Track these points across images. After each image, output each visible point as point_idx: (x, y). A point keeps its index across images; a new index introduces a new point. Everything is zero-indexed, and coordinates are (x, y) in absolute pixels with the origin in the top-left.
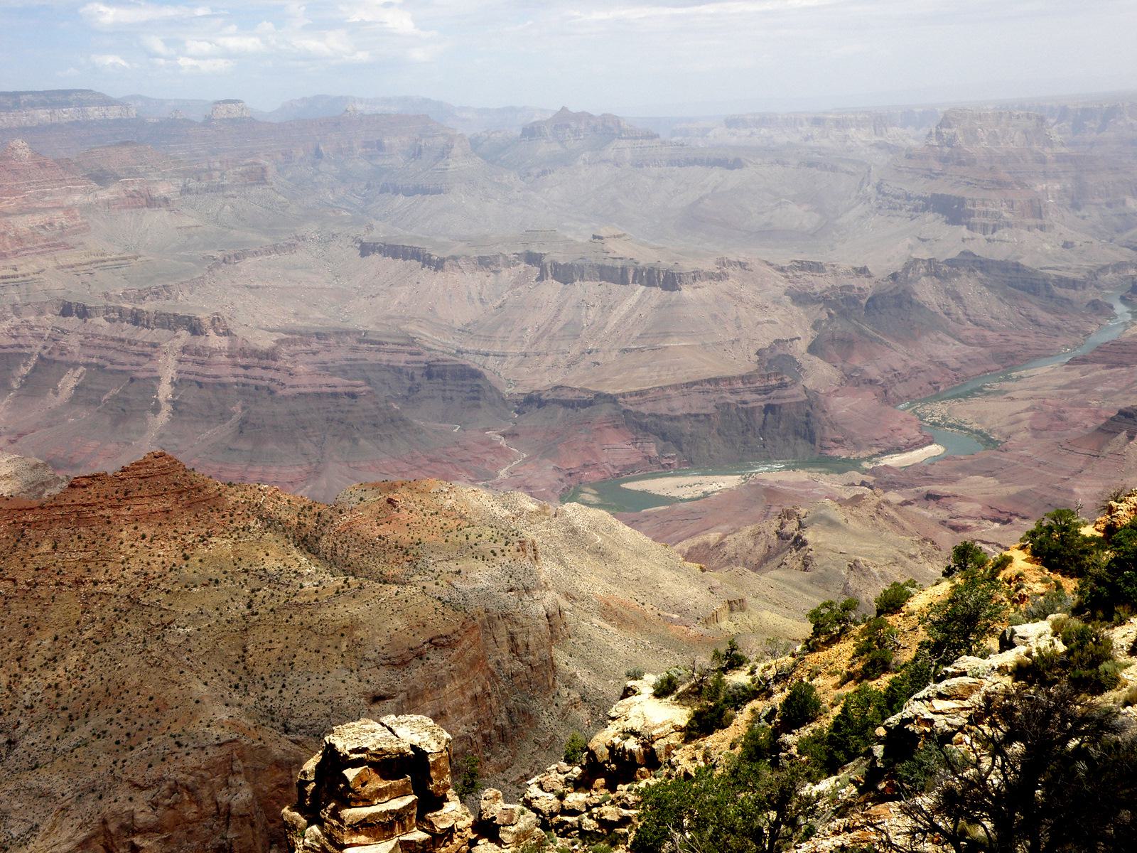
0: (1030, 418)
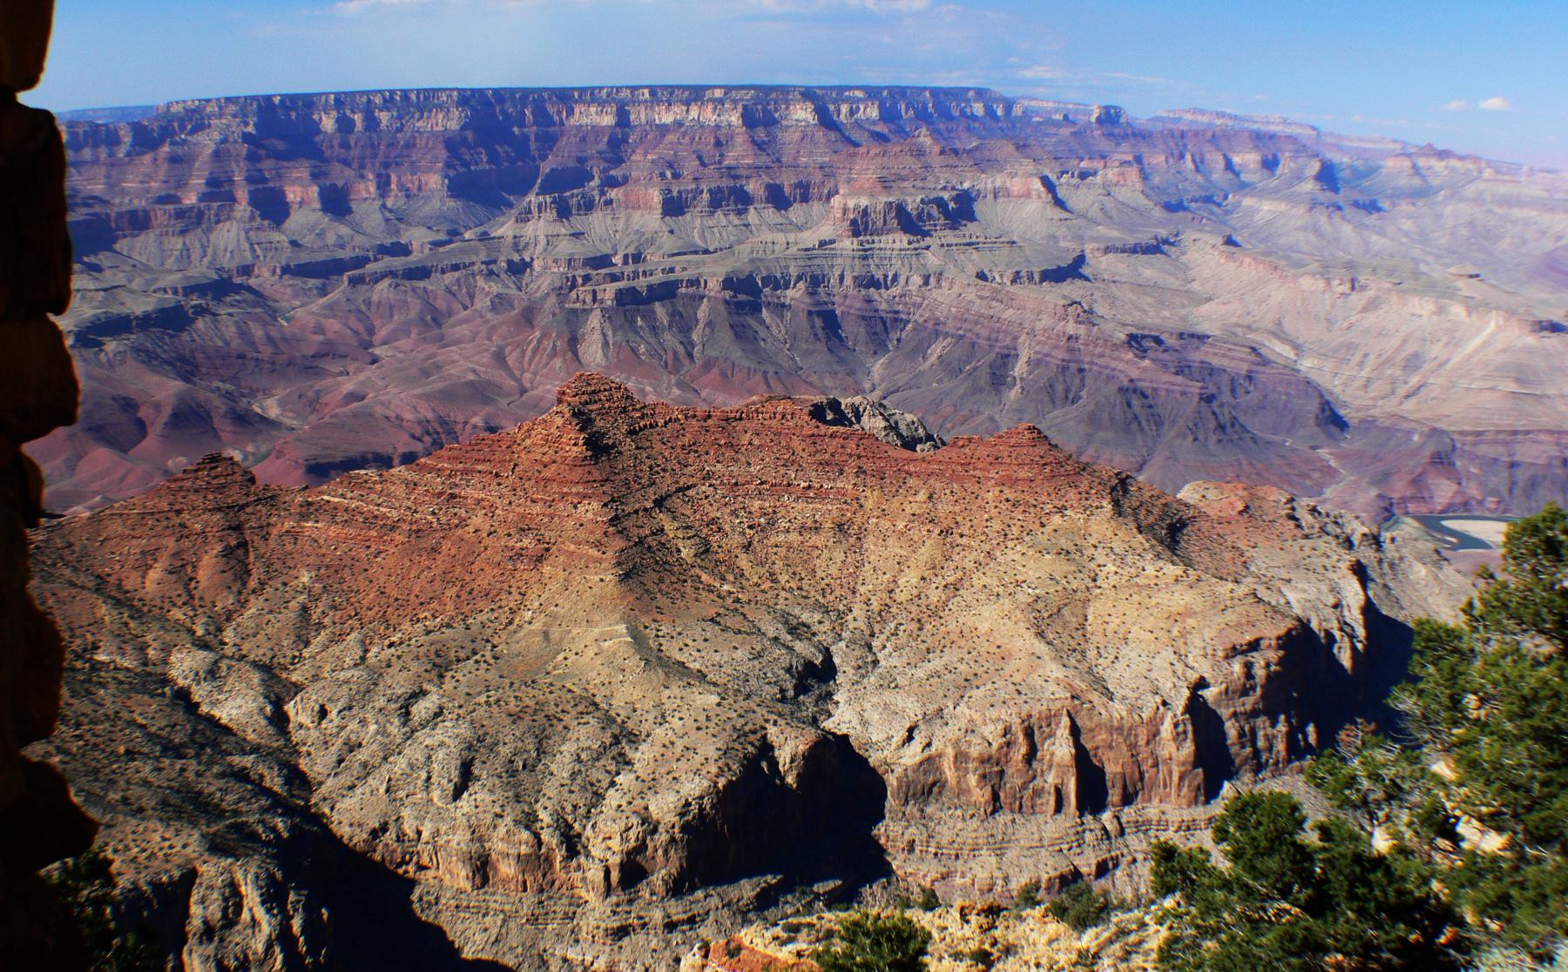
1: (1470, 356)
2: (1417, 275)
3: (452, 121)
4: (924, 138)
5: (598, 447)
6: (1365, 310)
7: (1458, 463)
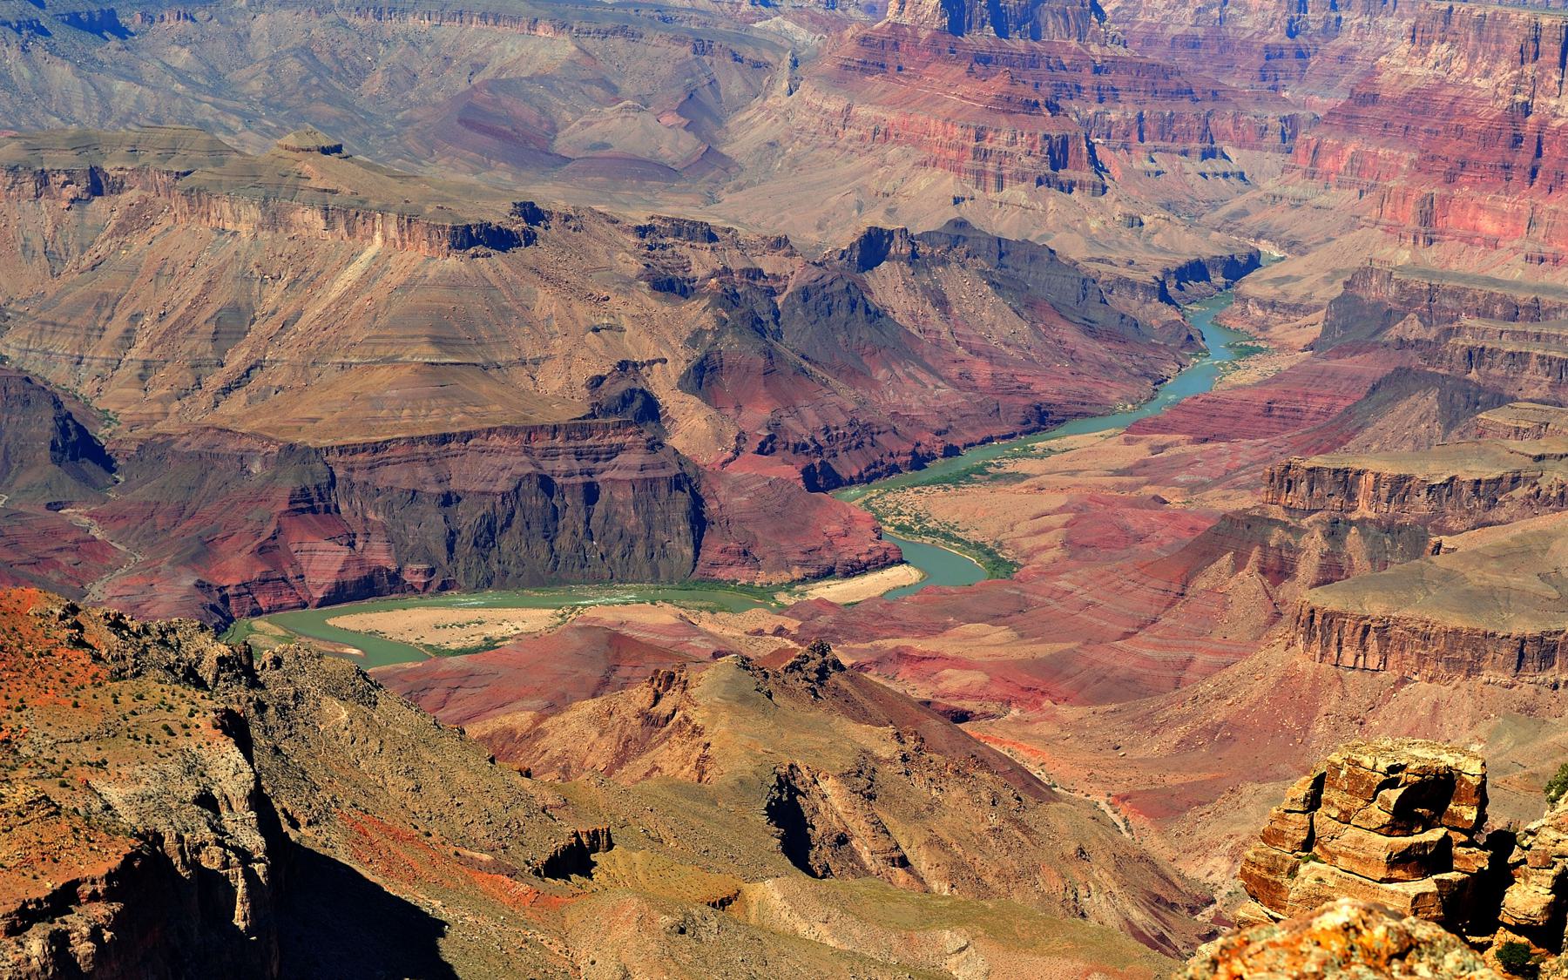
0: (1066, 526)
1: (343, 301)
2: (217, 153)
6: (123, 229)
7: (343, 507)
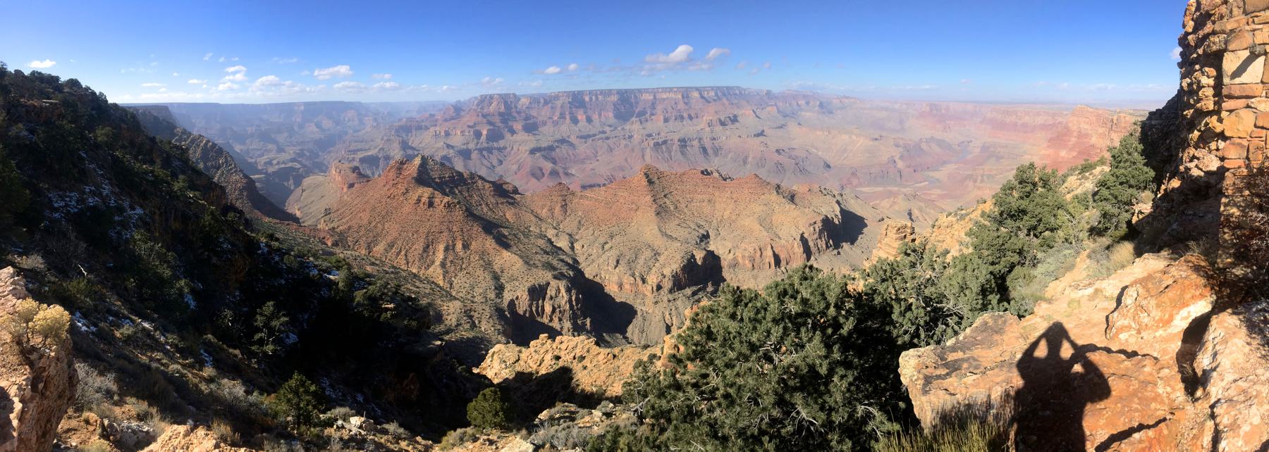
3: (615, 98)
4: (724, 100)
5: (650, 182)
